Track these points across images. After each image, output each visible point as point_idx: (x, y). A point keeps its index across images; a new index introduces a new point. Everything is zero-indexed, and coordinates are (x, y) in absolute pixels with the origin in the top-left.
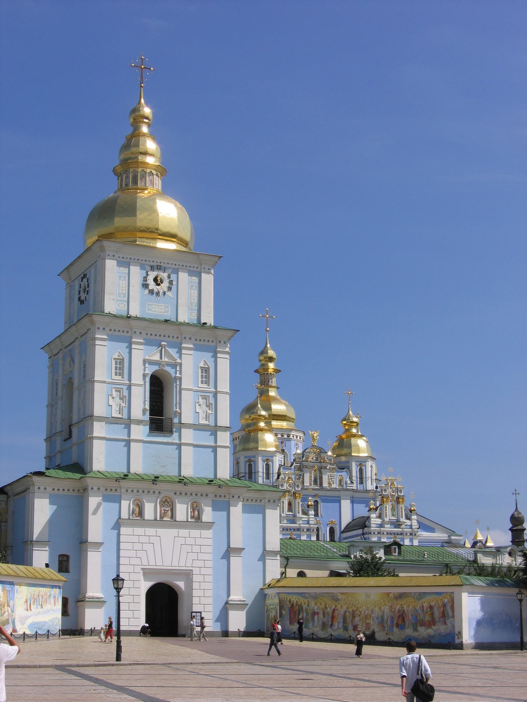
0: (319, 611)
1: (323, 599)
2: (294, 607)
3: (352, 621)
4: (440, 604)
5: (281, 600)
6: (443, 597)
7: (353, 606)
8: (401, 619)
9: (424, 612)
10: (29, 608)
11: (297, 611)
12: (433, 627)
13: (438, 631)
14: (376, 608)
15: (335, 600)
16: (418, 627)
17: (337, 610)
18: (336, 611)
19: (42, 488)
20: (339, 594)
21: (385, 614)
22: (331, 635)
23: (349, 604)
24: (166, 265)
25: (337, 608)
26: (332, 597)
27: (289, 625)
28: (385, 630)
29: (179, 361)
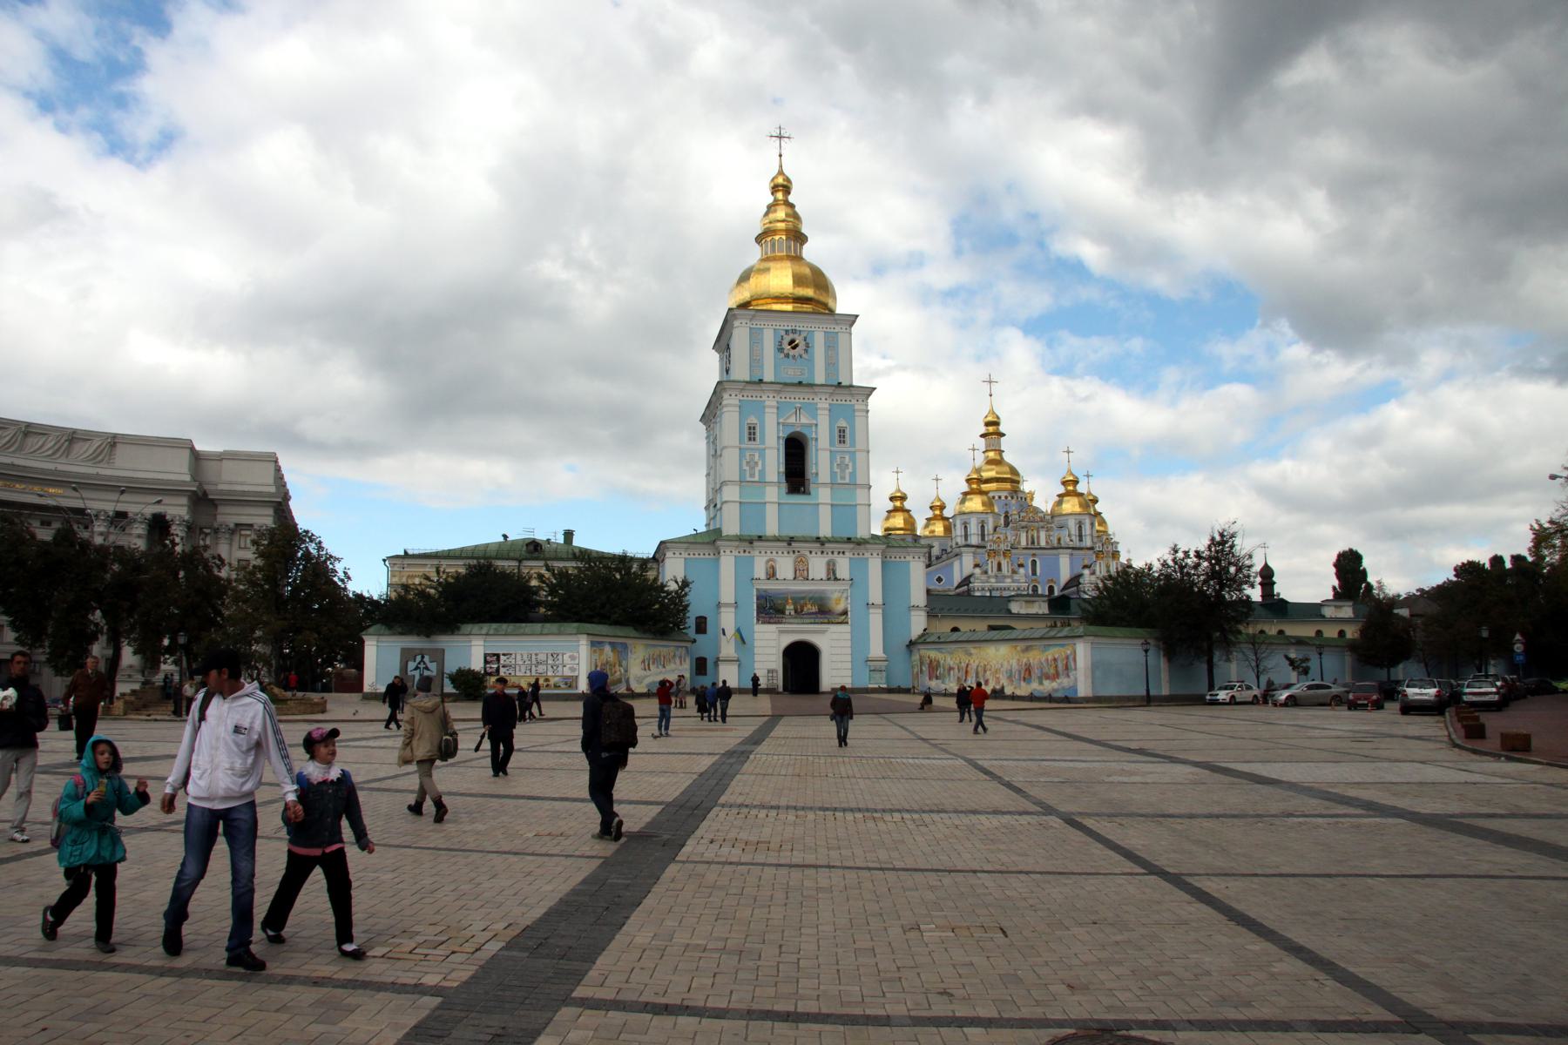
8: (1027, 672)
10: (647, 668)
15: (967, 654)
19: (677, 553)
24: (801, 329)
28: (1012, 684)
29: (815, 422)
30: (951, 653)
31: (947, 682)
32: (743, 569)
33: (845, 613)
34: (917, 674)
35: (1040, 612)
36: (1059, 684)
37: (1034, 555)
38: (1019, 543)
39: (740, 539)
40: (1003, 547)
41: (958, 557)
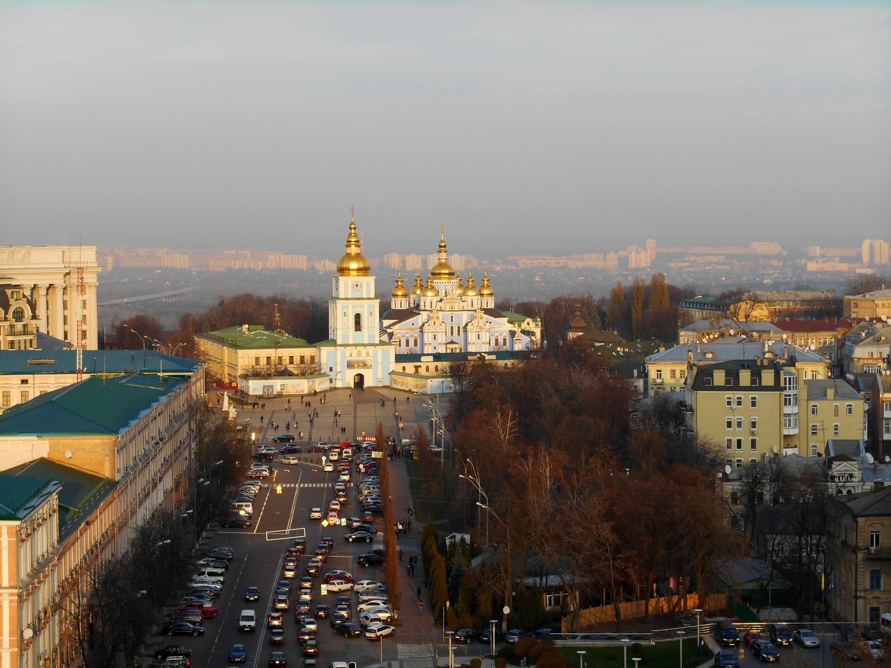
32: (343, 354)
33: (371, 366)
38: (446, 309)
39: (342, 345)
40: (436, 315)
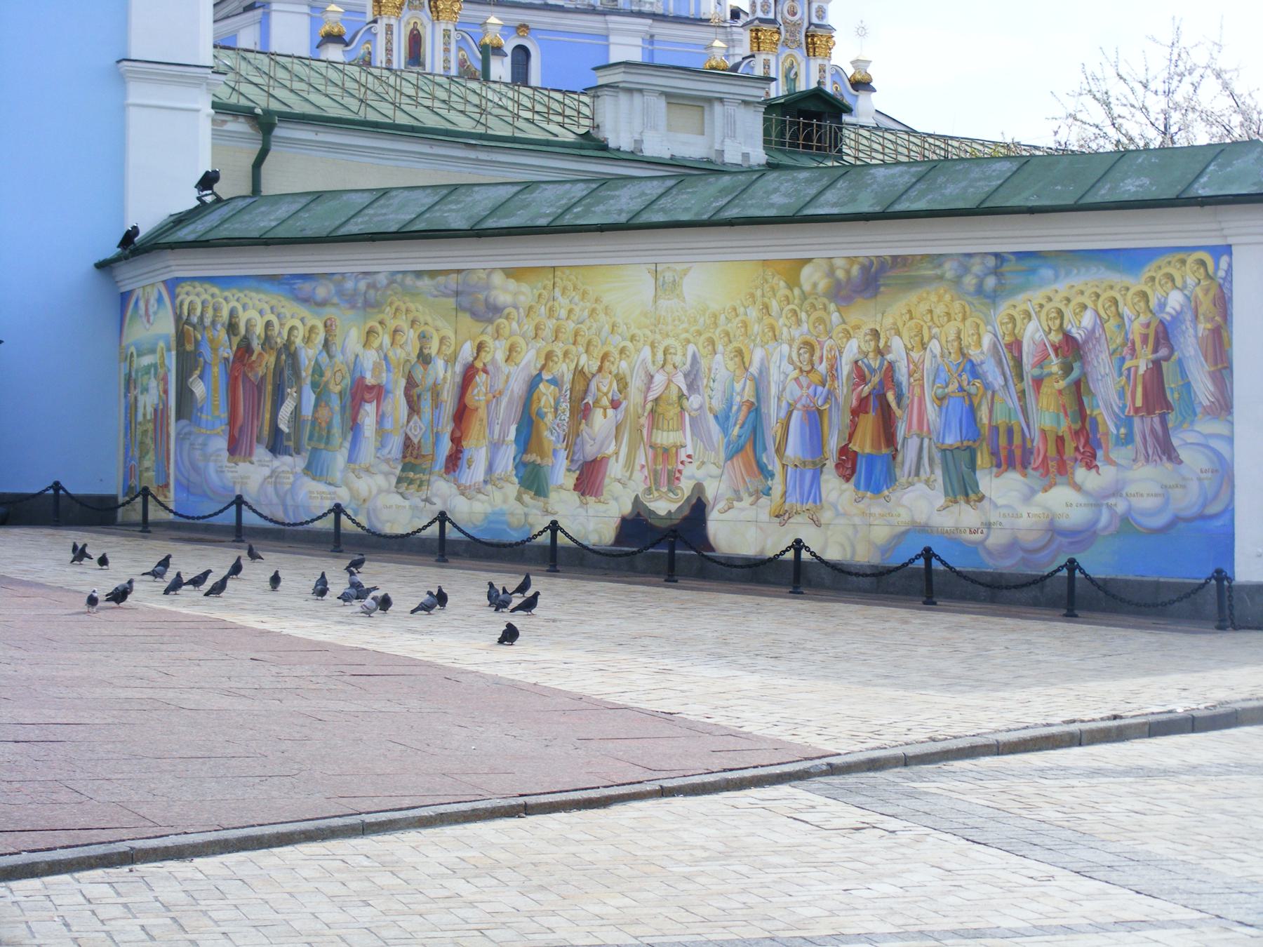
0: (384, 378)
1: (408, 310)
2: (254, 358)
3: (572, 439)
4: (1136, 329)
5: (188, 322)
6: (1153, 279)
7: (582, 349)
8: (868, 422)
9: (1020, 377)
11: (270, 379)
12: (1081, 474)
13: (1112, 501)
14: (719, 357)
15: (474, 315)
16: (979, 474)
17: (485, 371)
18: (480, 378)
20: (498, 279)
21: (774, 390)
22: (442, 518)
23: (557, 331)
25: (486, 357)
26: (457, 294)
27: (225, 463)
28: (767, 492)
30: (370, 305)
31: (338, 475)
34: (160, 415)
35: (732, 156)
36: (1098, 500)
37: (523, 28)
41: (258, 13)
